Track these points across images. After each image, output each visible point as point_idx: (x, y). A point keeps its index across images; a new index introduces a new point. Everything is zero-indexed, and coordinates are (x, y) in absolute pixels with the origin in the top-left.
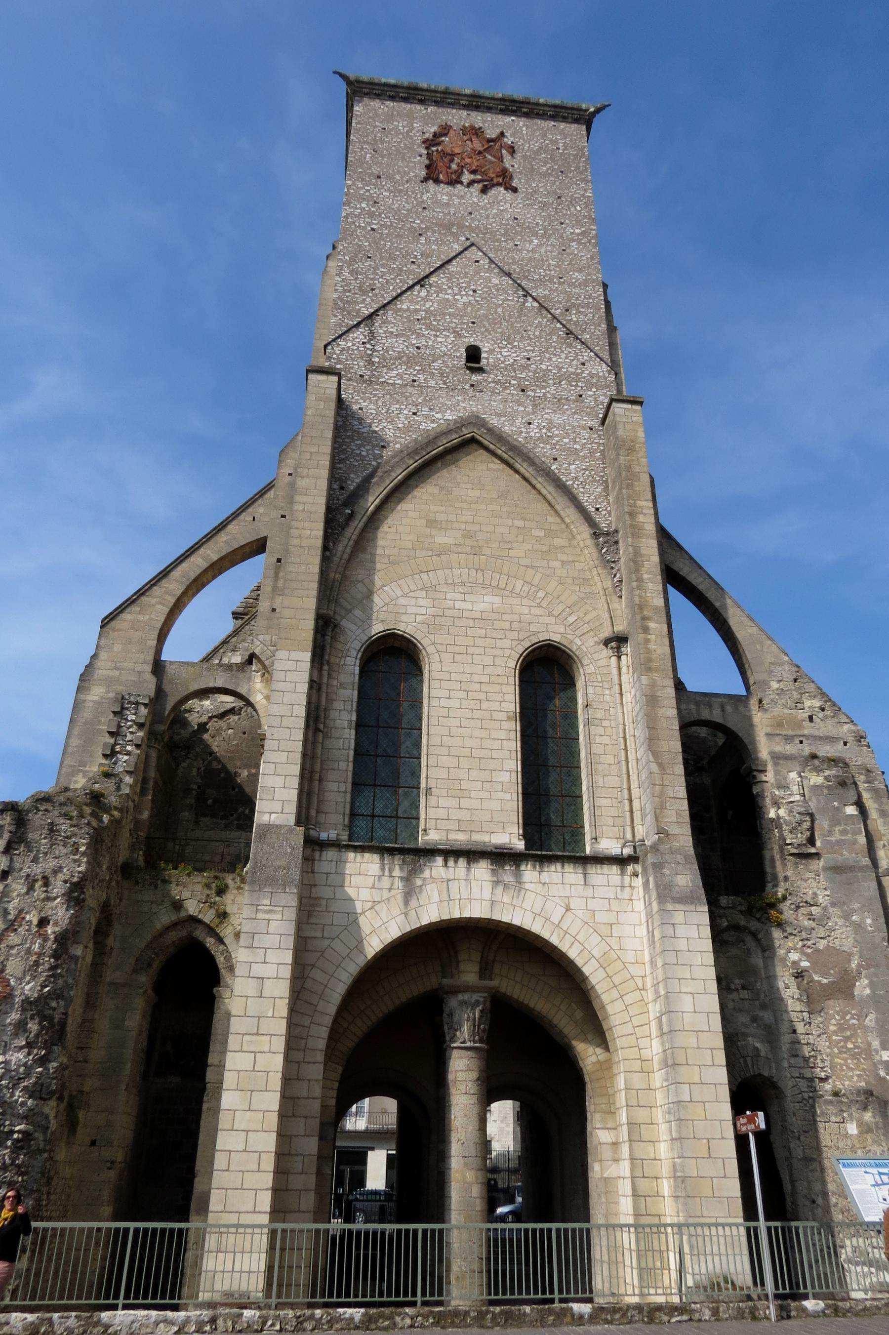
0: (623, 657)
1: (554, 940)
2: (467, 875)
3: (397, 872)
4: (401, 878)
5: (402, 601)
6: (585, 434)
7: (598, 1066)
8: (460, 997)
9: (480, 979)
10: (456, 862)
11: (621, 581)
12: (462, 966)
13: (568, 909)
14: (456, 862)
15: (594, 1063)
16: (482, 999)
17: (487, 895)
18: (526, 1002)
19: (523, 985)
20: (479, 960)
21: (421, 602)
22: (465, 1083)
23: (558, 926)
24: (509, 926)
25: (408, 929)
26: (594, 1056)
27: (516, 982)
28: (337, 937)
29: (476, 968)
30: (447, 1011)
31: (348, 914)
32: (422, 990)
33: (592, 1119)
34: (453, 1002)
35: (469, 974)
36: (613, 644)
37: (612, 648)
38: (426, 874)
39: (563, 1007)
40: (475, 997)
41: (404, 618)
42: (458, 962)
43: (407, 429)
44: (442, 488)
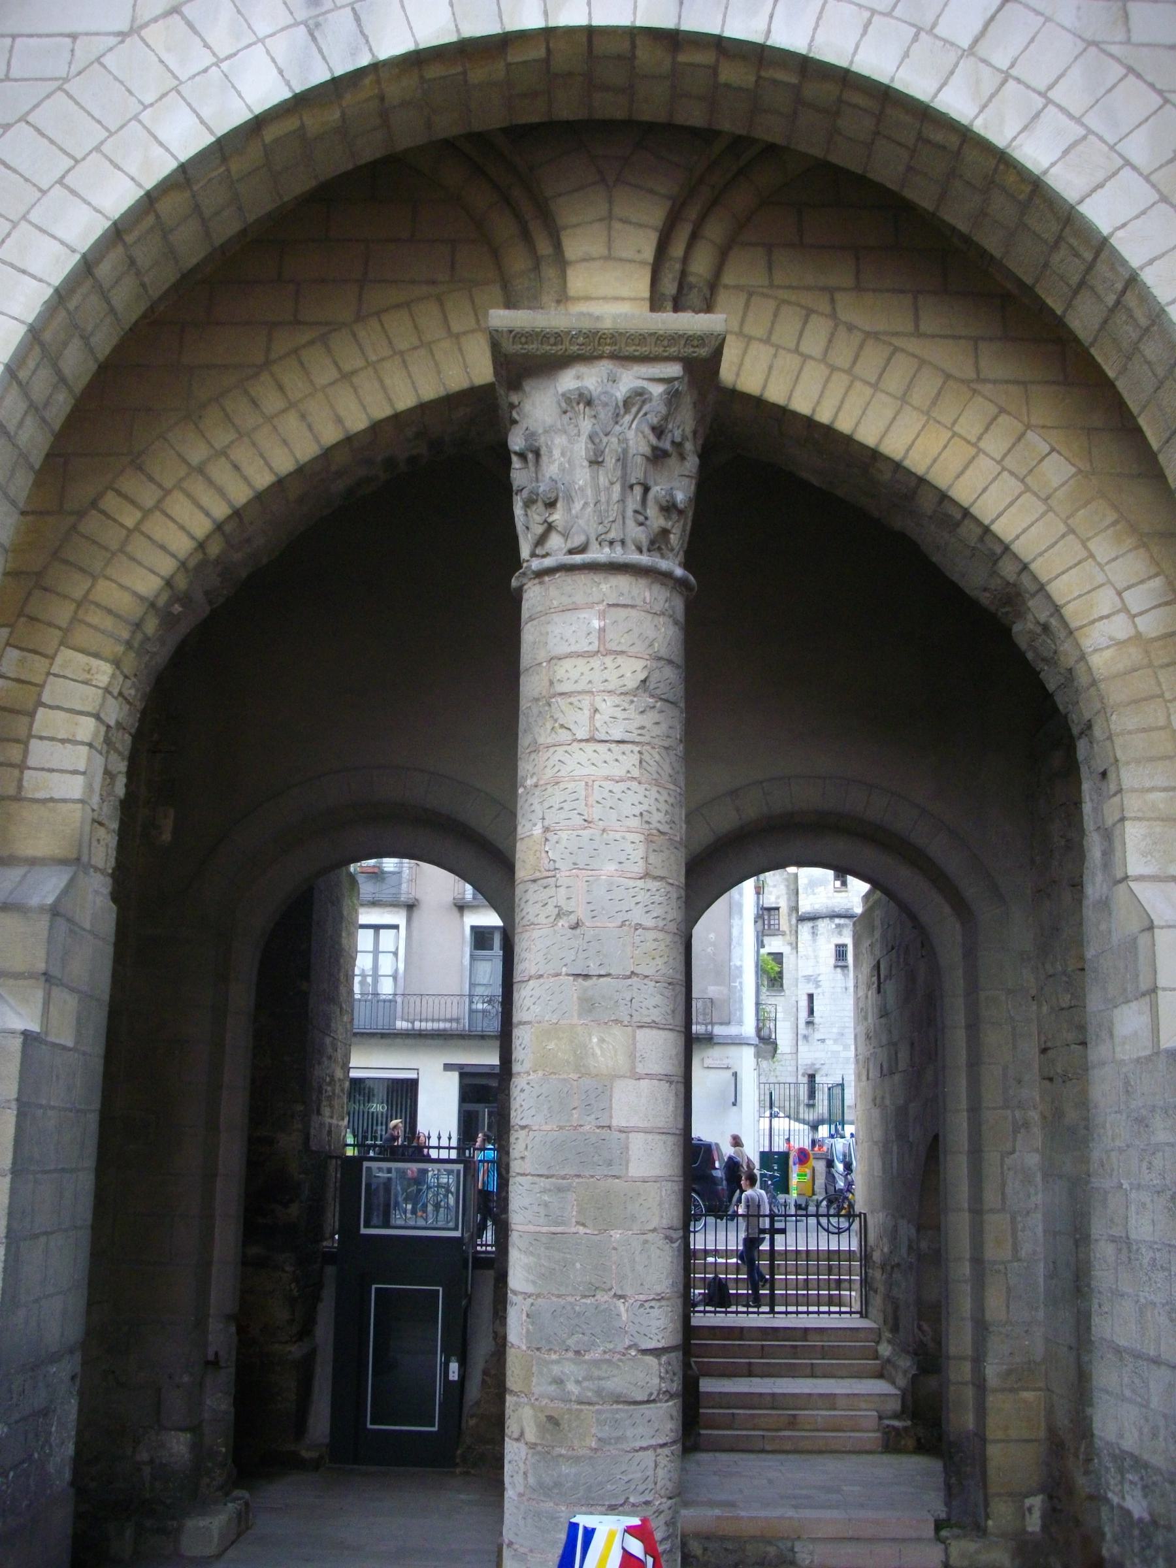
1: (956, 103)
7: (1135, 654)
8: (568, 381)
9: (655, 303)
12: (578, 280)
15: (1120, 644)
16: (657, 390)
18: (844, 425)
19: (833, 369)
20: (649, 254)
22: (586, 701)
23: (971, 50)
24: (758, 55)
25: (320, 76)
26: (1121, 619)
27: (806, 357)
28: (23, 119)
29: (641, 285)
30: (516, 442)
31: (74, 37)
32: (430, 391)
33: (1108, 853)
34: (540, 409)
35: (606, 283)
39: (995, 444)
40: (630, 379)
42: (562, 263)
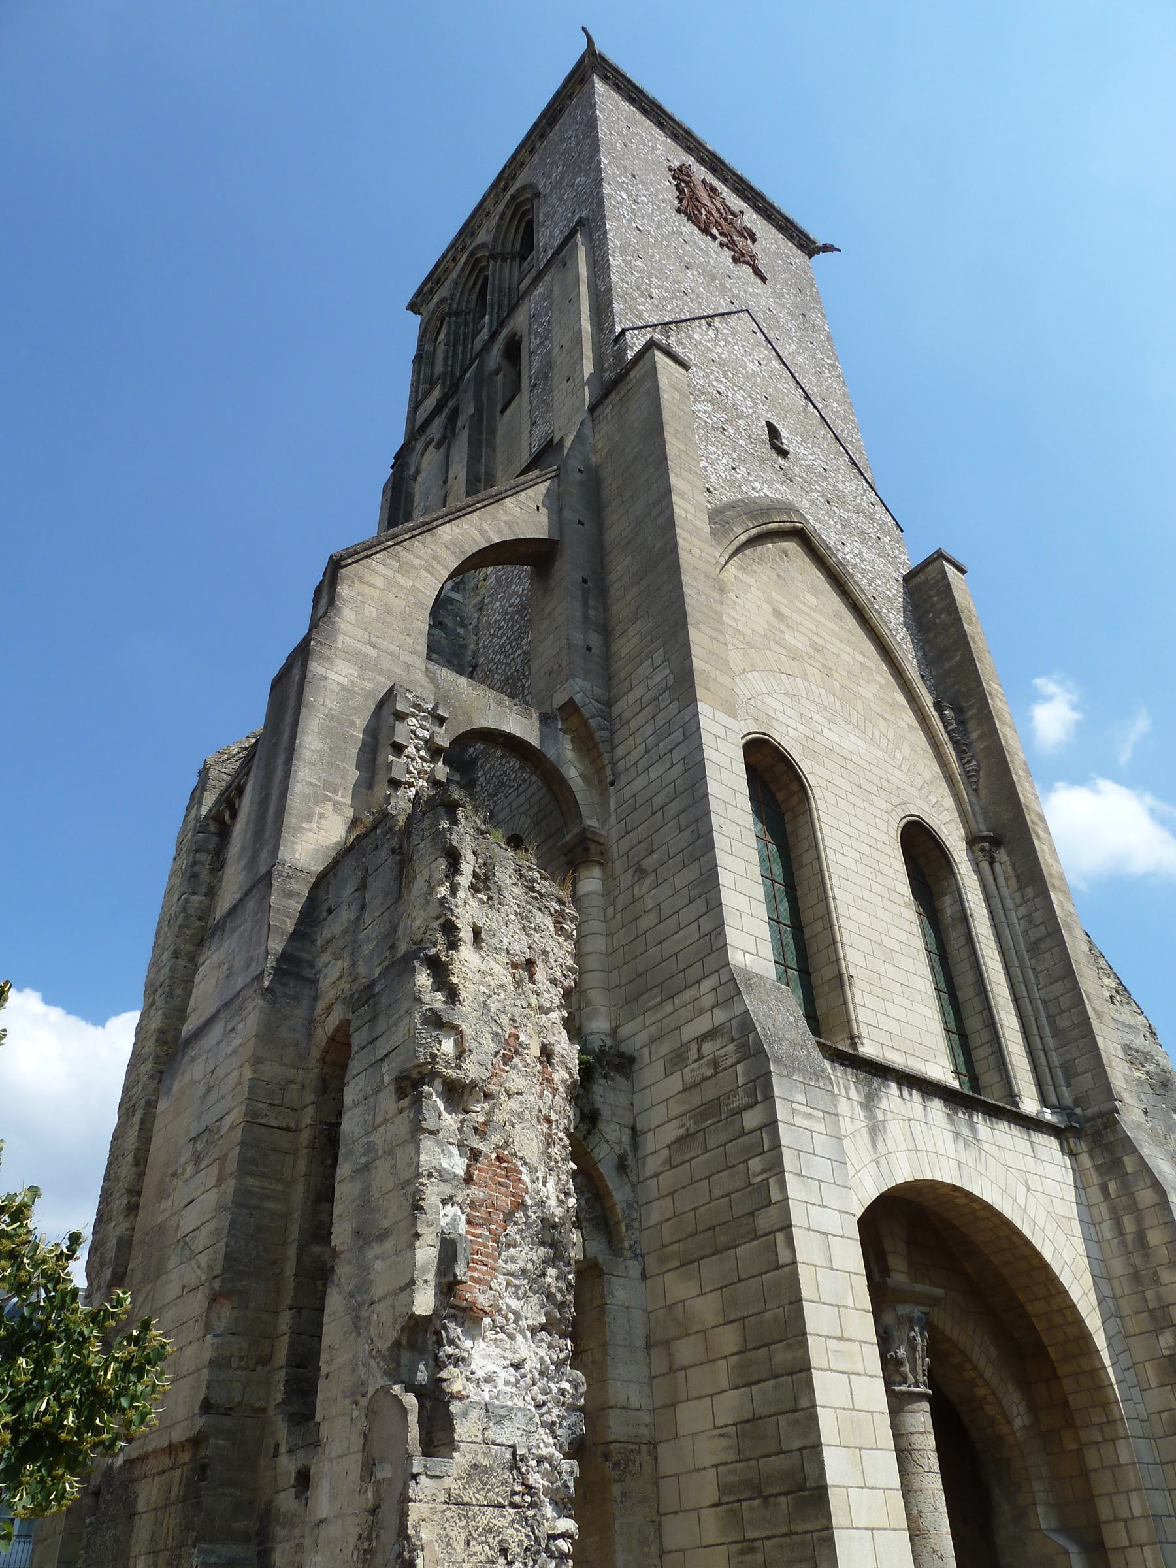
0: (997, 866)
2: (926, 1116)
3: (853, 1094)
4: (861, 1103)
5: (768, 699)
6: (892, 582)
10: (911, 1094)
11: (978, 771)
13: (1029, 1190)
14: (911, 1094)
17: (952, 1154)
21: (789, 712)
36: (986, 845)
37: (982, 850)
38: (884, 1104)
41: (775, 724)
43: (730, 482)
44: (779, 576)
